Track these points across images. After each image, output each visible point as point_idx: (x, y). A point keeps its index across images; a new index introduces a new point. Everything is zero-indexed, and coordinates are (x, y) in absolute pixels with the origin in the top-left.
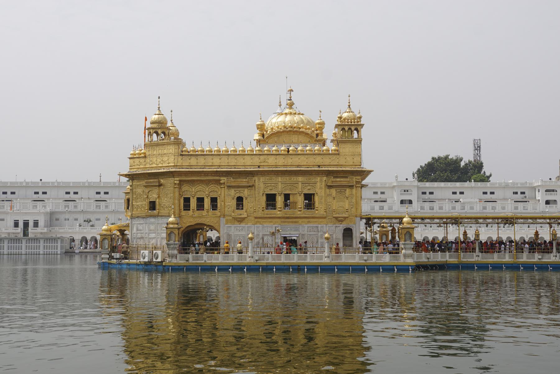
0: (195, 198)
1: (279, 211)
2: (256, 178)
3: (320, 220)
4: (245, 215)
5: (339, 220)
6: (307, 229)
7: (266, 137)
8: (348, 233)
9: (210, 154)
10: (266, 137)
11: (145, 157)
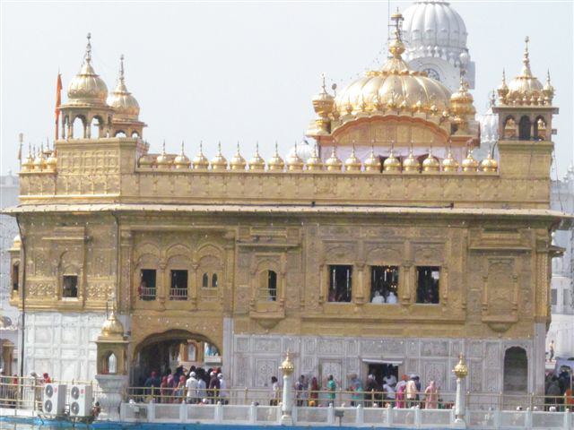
0: (168, 272)
1: (358, 305)
2: (304, 229)
3: (452, 328)
4: (280, 315)
5: (497, 329)
6: (423, 348)
7: (335, 127)
8: (515, 360)
9: (204, 172)
10: (335, 127)
11: (55, 174)
